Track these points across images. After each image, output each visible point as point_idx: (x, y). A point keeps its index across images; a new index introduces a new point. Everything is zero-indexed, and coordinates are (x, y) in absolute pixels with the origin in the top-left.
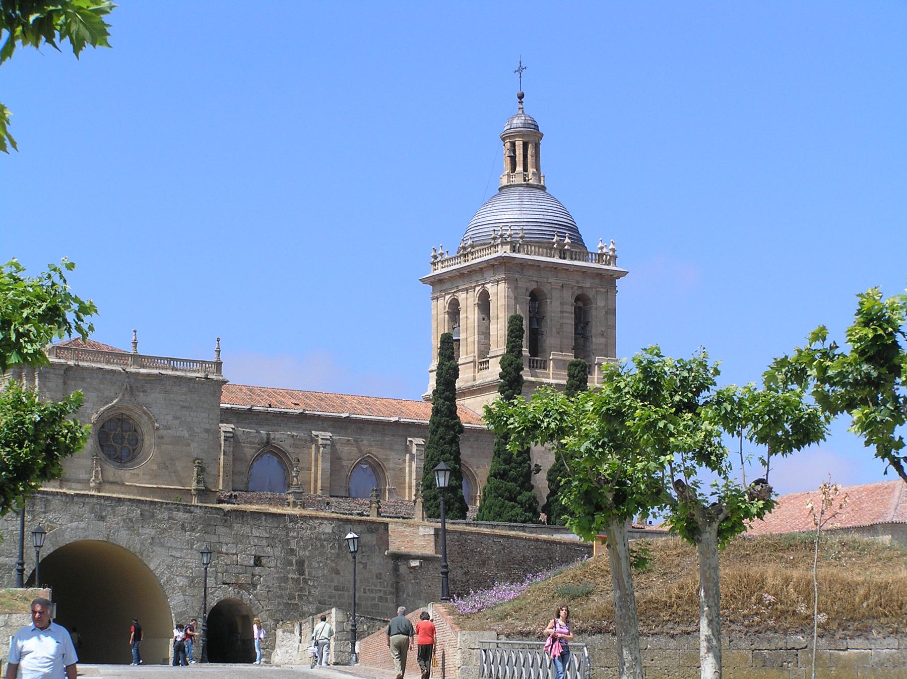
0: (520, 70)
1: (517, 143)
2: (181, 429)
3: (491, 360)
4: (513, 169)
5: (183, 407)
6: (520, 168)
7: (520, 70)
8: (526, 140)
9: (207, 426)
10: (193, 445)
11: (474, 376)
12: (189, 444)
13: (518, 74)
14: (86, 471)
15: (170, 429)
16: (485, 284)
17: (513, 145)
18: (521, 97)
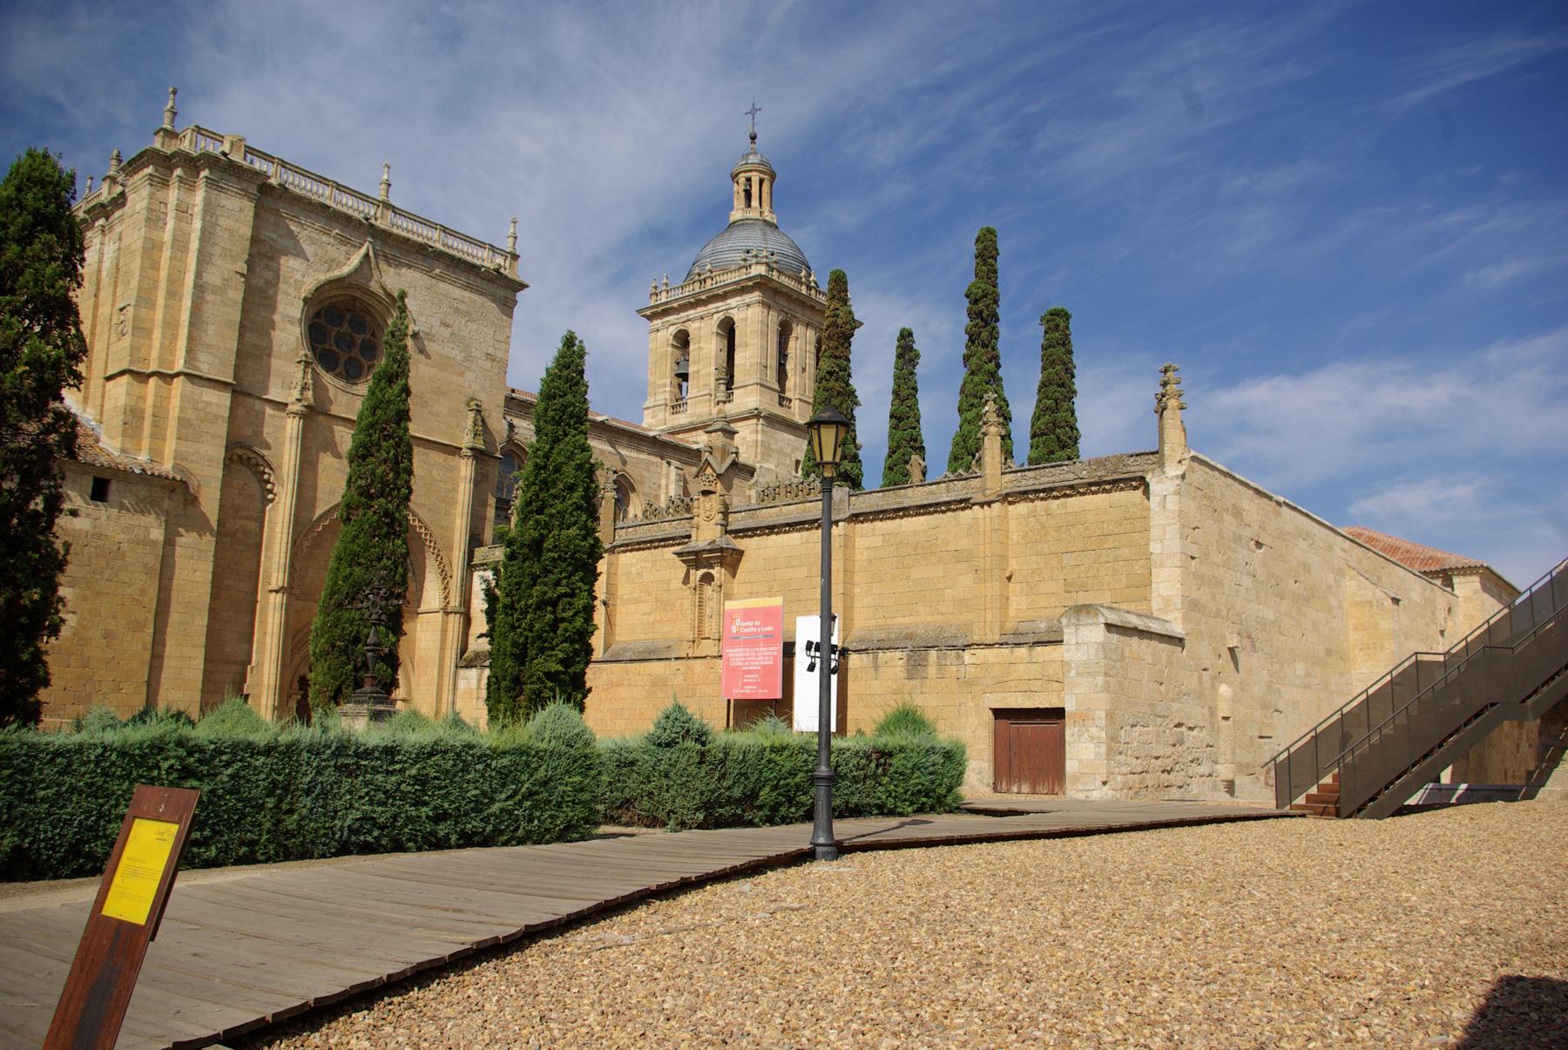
0: (753, 112)
1: (753, 179)
2: (452, 345)
3: (736, 392)
4: (749, 205)
5: (457, 310)
6: (755, 203)
7: (753, 112)
8: (762, 176)
9: (491, 351)
10: (470, 376)
11: (710, 410)
12: (463, 373)
13: (750, 116)
14: (283, 382)
15: (434, 341)
16: (727, 310)
17: (749, 180)
18: (753, 138)
